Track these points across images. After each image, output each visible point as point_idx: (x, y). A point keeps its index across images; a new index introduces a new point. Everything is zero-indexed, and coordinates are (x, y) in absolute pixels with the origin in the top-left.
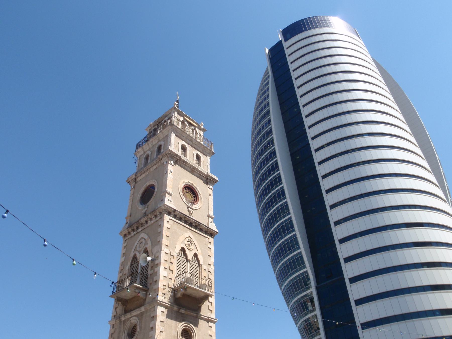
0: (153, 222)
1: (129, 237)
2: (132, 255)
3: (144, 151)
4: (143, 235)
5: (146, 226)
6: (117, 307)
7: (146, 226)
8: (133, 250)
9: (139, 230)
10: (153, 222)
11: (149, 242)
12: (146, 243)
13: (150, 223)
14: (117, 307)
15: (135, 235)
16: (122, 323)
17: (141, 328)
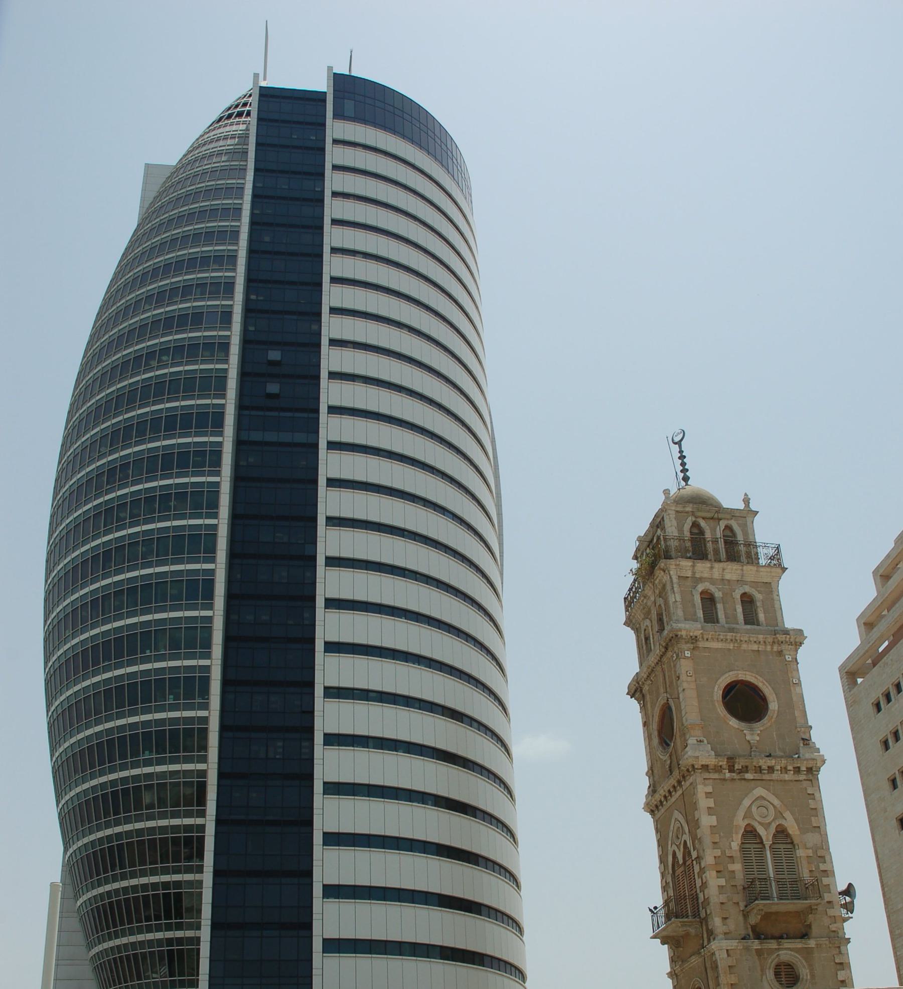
0: (787, 777)
1: (716, 776)
2: (741, 823)
3: (694, 573)
4: (760, 791)
5: (766, 777)
6: (726, 918)
7: (766, 777)
8: (741, 813)
9: (749, 776)
10: (787, 777)
11: (787, 814)
12: (779, 814)
13: (775, 776)
14: (726, 918)
15: (733, 780)
16: (754, 952)
17: (813, 976)
